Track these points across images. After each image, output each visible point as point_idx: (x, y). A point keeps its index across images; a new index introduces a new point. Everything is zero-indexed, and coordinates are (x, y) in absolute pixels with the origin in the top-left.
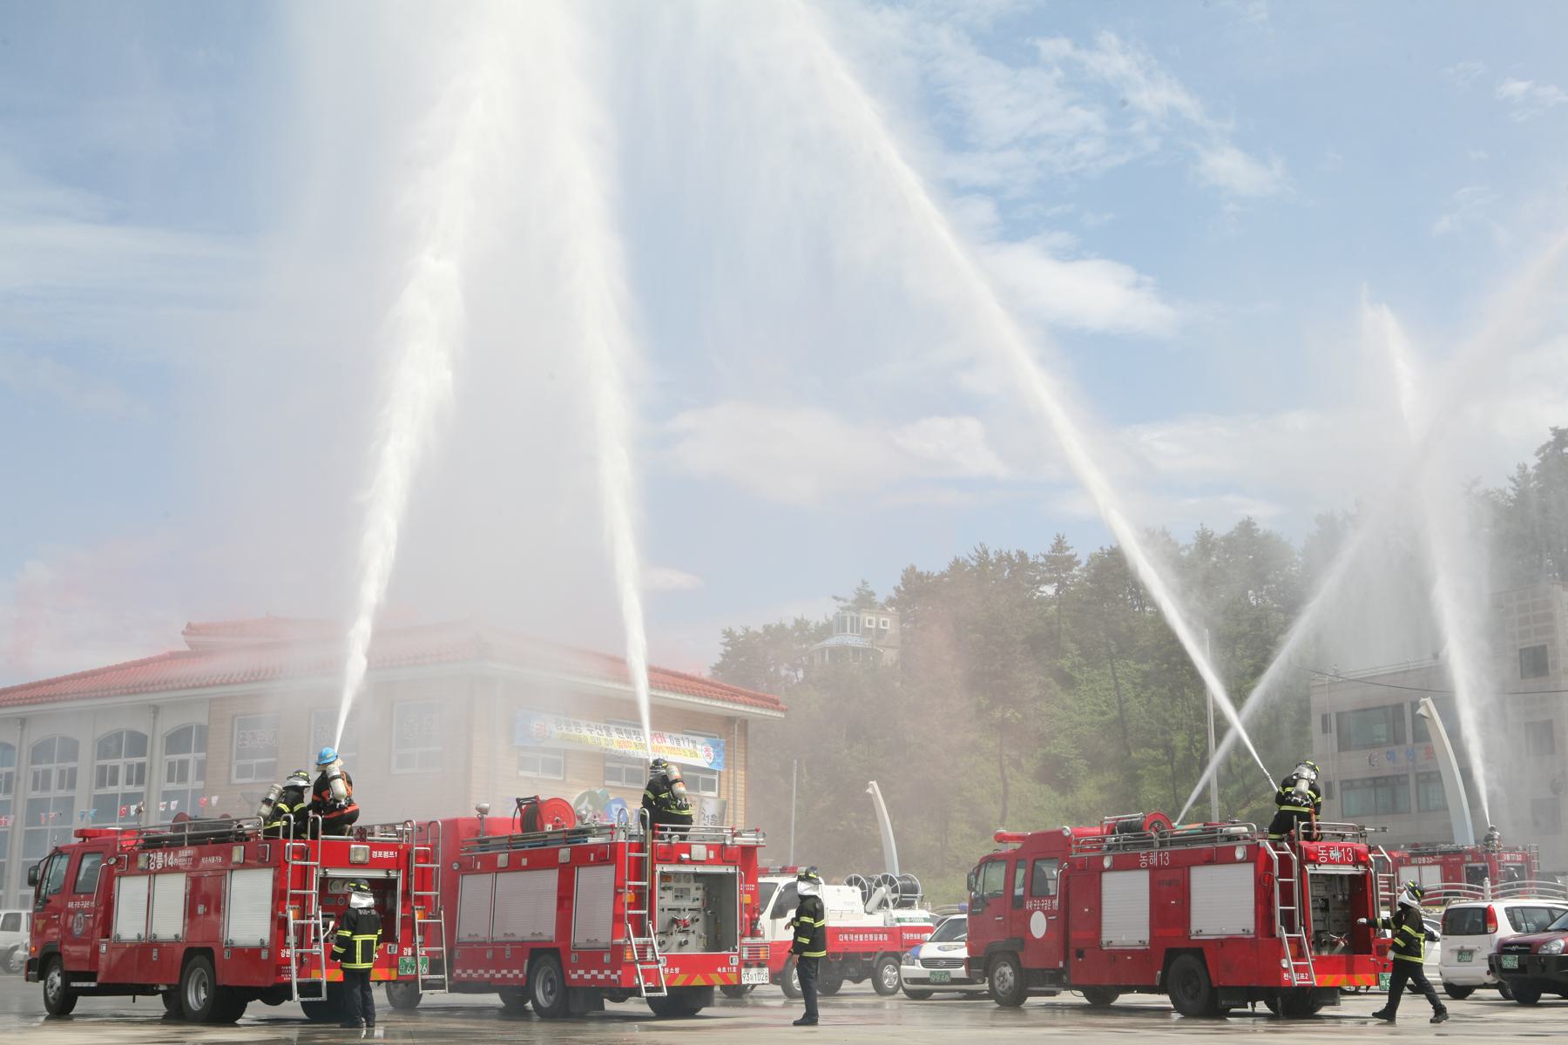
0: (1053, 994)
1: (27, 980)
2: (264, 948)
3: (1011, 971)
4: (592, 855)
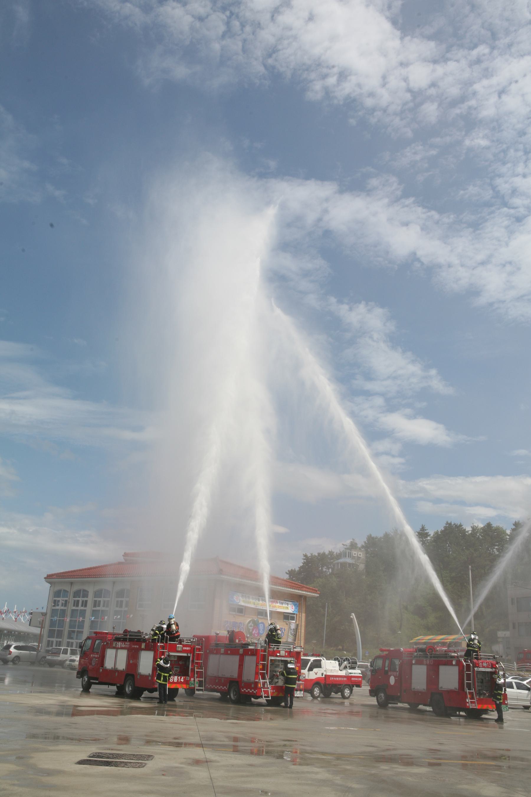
0: (397, 704)
2: (150, 676)
4: (250, 652)
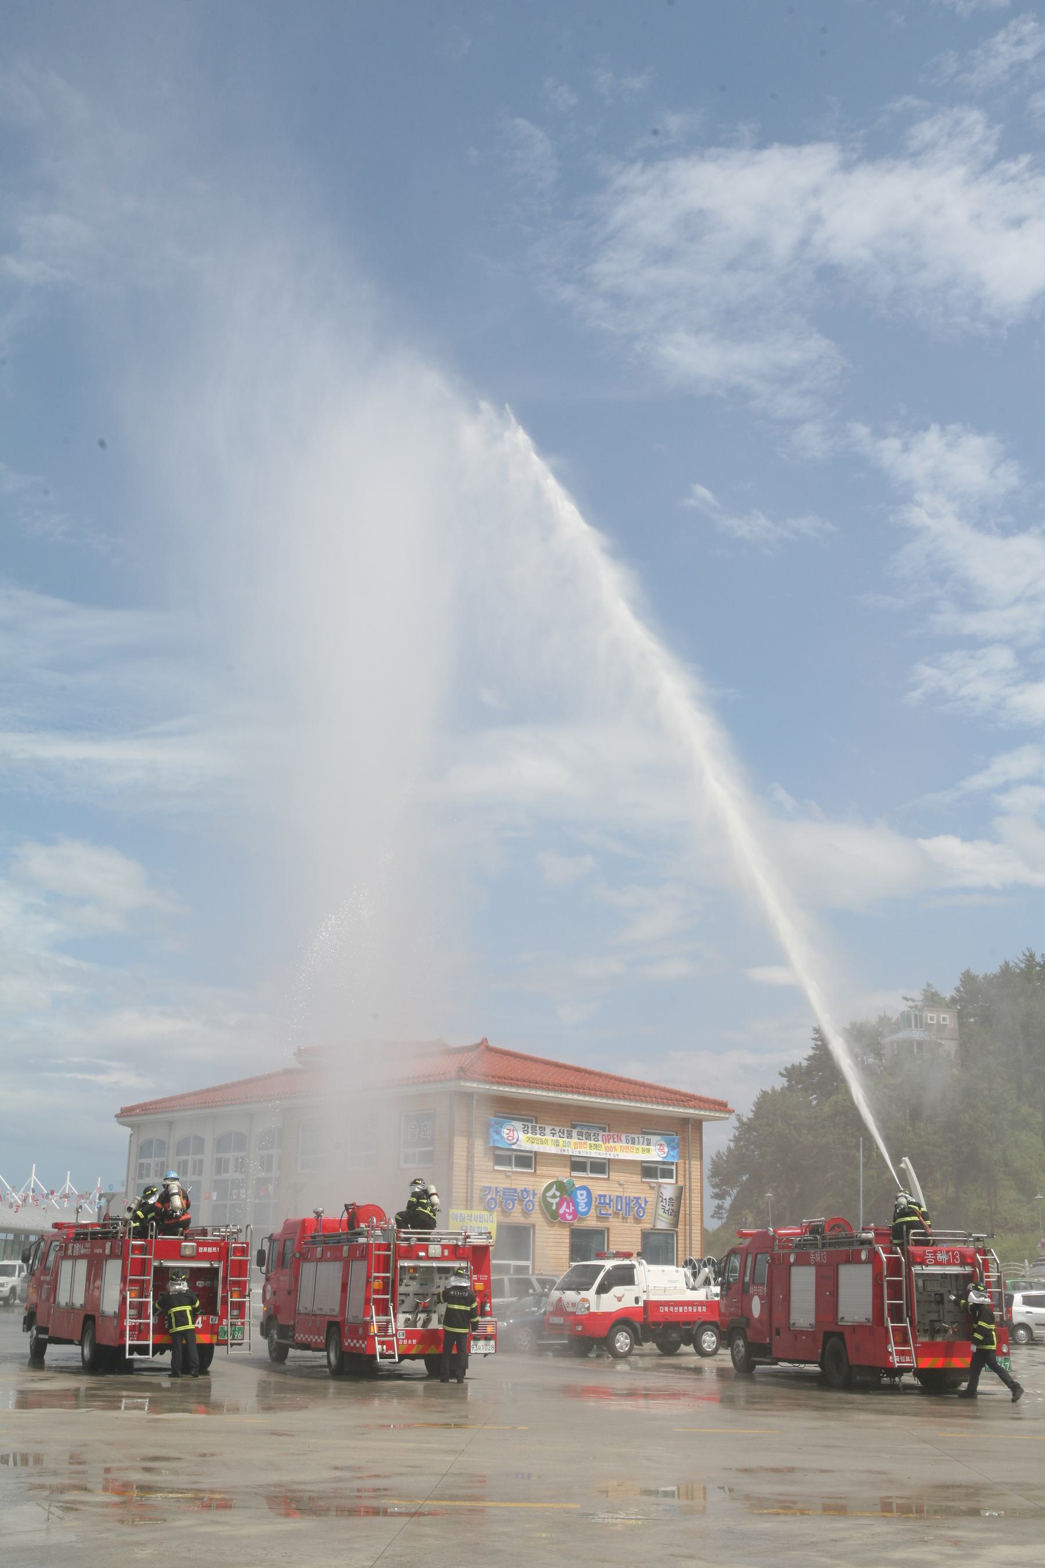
1: (24, 1331)
3: (743, 1344)
